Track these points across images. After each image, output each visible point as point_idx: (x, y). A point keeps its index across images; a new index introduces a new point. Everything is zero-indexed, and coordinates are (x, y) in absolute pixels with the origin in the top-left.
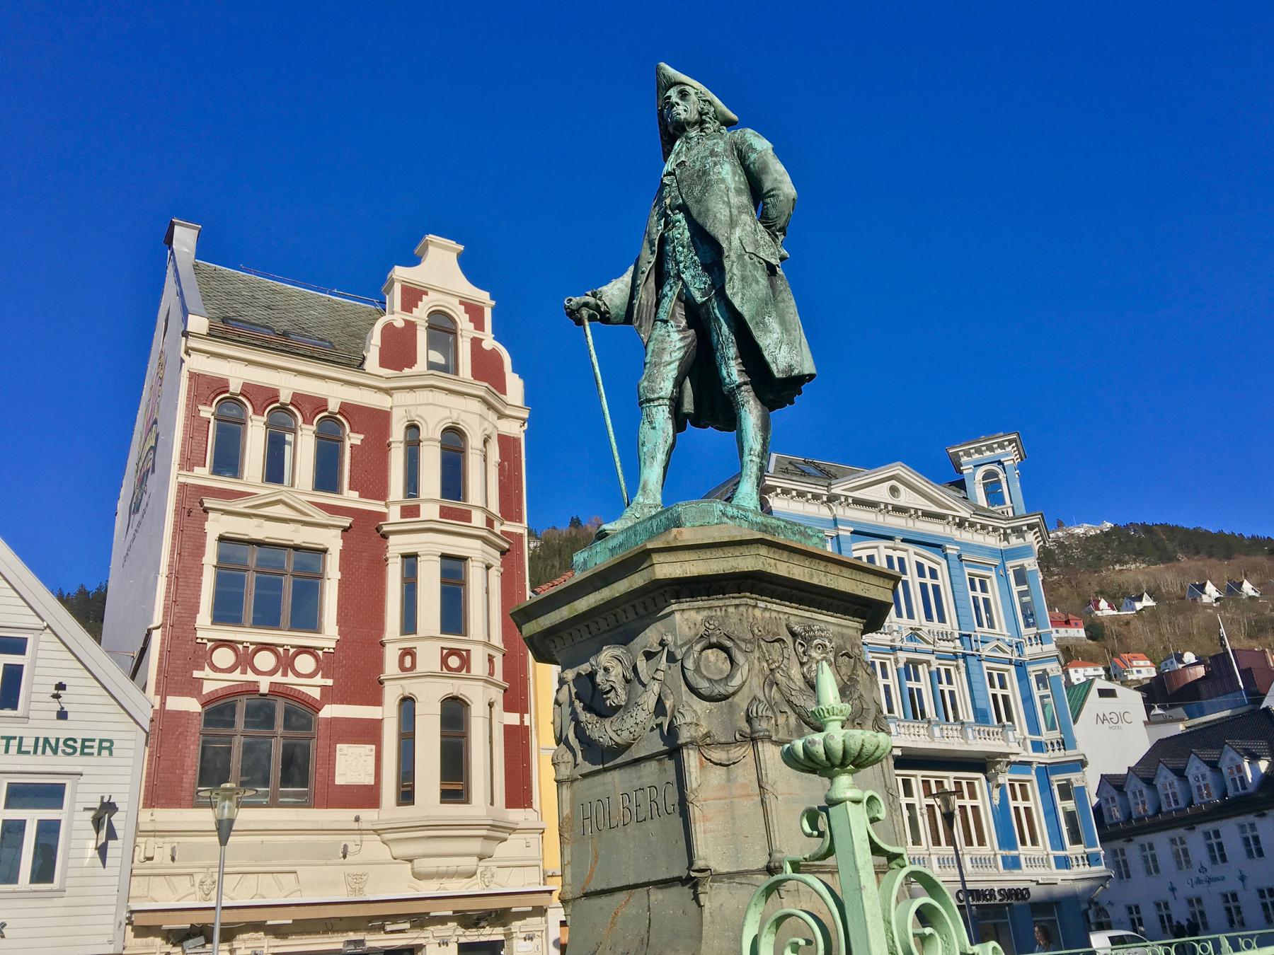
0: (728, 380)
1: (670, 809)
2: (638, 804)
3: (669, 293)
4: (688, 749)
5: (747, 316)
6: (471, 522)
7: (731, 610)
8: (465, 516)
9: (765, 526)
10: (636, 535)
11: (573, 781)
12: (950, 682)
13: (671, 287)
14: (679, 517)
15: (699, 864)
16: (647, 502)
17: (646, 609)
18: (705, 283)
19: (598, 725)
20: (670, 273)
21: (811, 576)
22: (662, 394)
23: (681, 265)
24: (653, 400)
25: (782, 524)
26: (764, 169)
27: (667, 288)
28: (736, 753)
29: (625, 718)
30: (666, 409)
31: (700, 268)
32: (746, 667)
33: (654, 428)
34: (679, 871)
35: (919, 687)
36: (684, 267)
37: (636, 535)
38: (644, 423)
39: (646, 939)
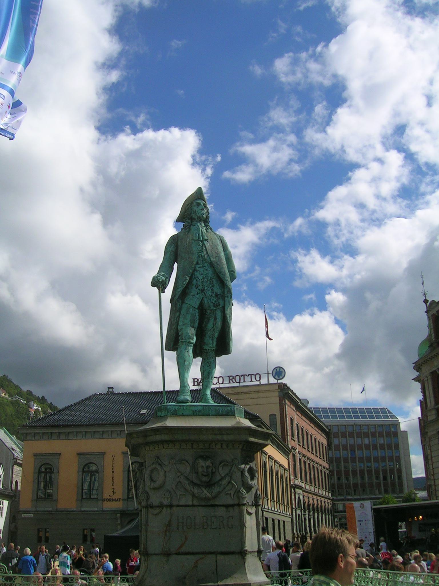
10: (209, 410)
13: (198, 294)
17: (227, 447)
18: (215, 301)
31: (214, 294)
39: (215, 572)
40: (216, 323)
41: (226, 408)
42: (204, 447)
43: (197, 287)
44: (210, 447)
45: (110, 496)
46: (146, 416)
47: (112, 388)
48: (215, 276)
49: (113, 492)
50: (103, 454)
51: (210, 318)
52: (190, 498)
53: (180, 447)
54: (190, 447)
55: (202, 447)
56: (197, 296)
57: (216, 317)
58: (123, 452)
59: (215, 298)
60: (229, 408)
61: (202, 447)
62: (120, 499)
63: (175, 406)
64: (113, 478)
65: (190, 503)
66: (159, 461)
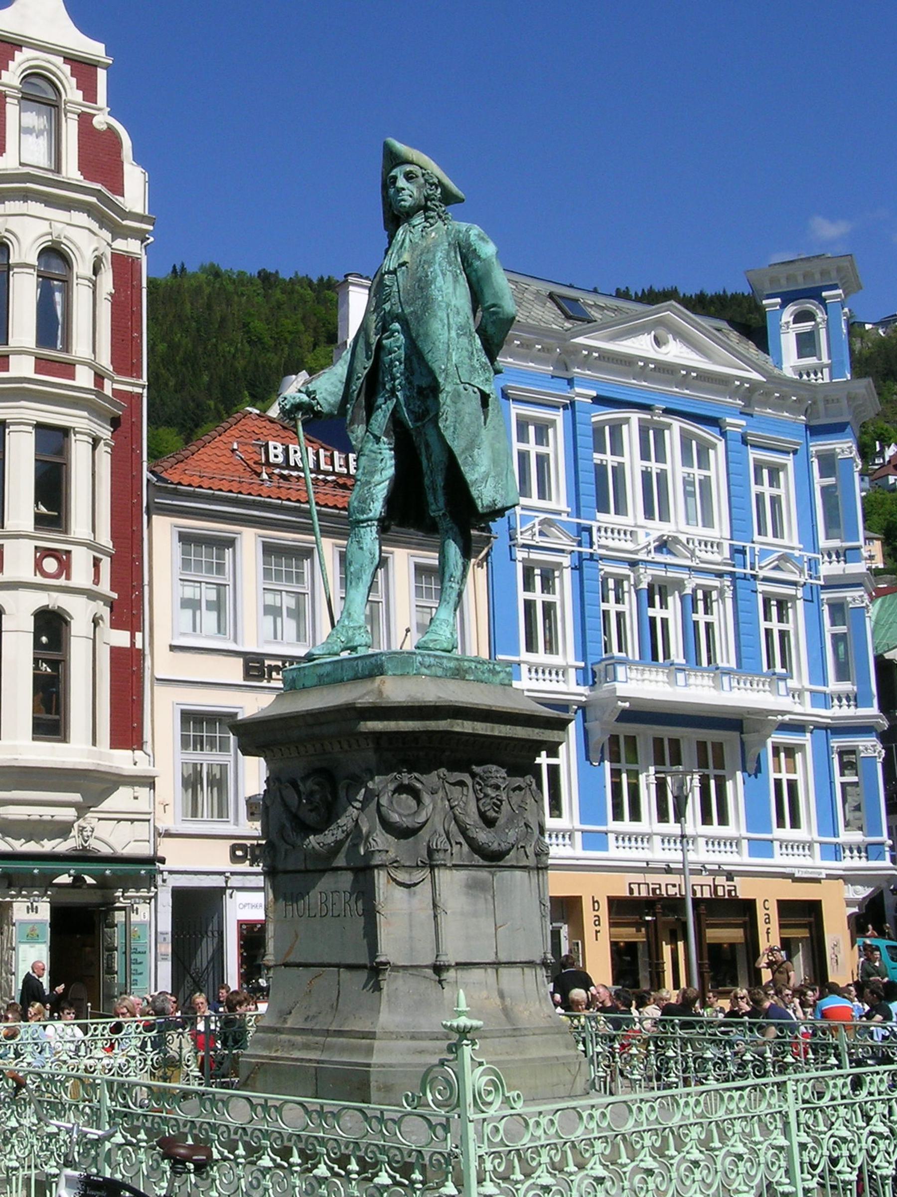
0: (433, 507)
3: (383, 406)
5: (457, 451)
6: (73, 378)
8: (67, 369)
9: (458, 670)
10: (342, 670)
12: (708, 610)
15: (382, 959)
16: (352, 625)
18: (419, 407)
20: (384, 385)
21: (492, 730)
22: (371, 515)
23: (397, 382)
24: (363, 521)
25: (473, 665)
26: (488, 274)
27: (380, 401)
28: (417, 875)
30: (374, 529)
32: (431, 807)
33: (361, 548)
34: (364, 960)
35: (665, 616)
37: (342, 670)
40: (431, 455)
57: (427, 440)
59: (419, 400)
65: (302, 867)
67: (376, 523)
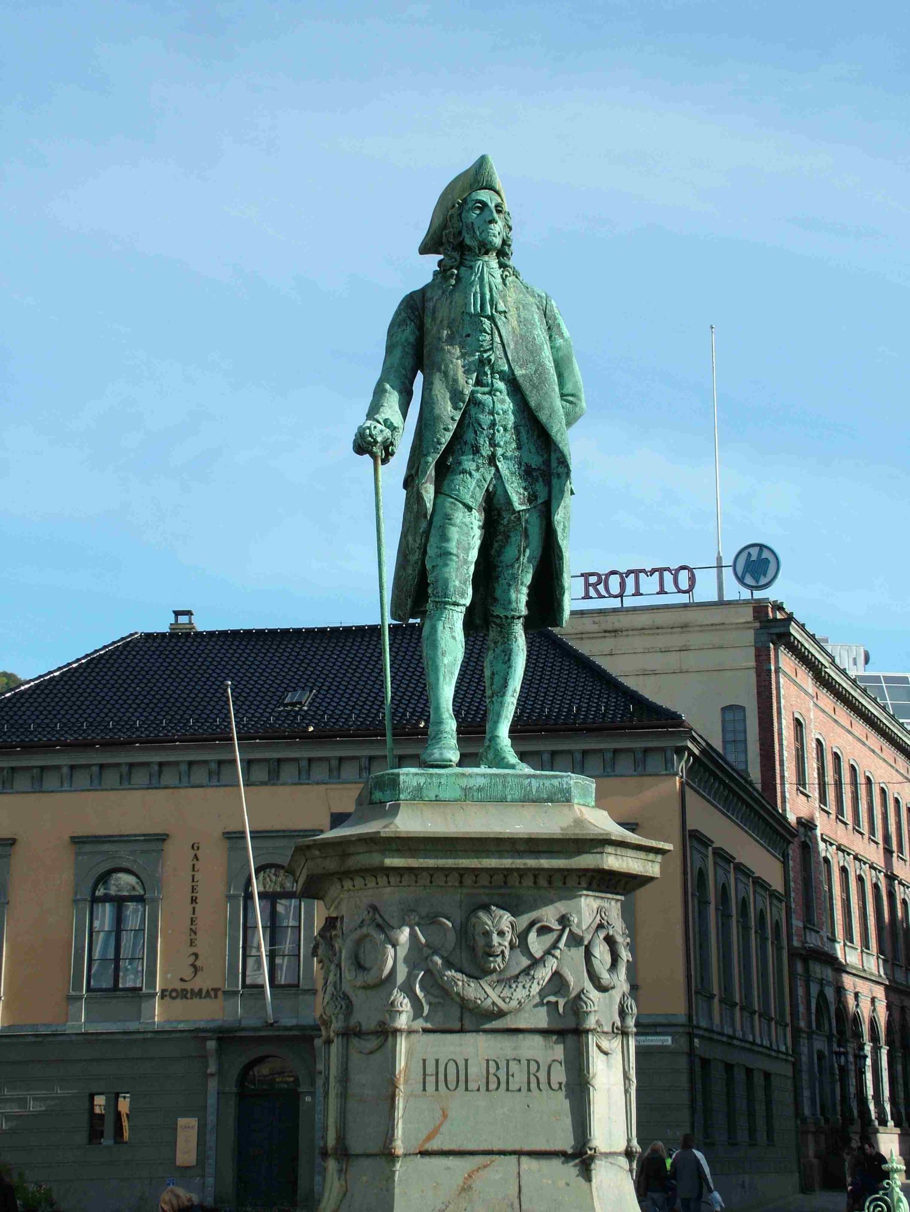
0: (514, 605)
1: (555, 1086)
2: (510, 1073)
4: (593, 1035)
7: (613, 903)
10: (504, 786)
11: (410, 1032)
14: (569, 791)
17: (550, 883)
19: (472, 985)
29: (514, 986)
36: (502, 455)
37: (504, 786)
38: (444, 628)
41: (547, 783)
42: (491, 883)
43: (476, 451)
44: (505, 883)
45: (182, 980)
46: (306, 711)
47: (189, 613)
48: (524, 418)
49: (193, 965)
50: (162, 838)
51: (512, 534)
52: (456, 1012)
53: (431, 882)
54: (457, 884)
55: (487, 884)
56: (477, 475)
58: (228, 833)
60: (555, 782)
61: (487, 884)
62: (216, 990)
63: (418, 777)
64: (192, 921)
66: (377, 916)
67: (464, 609)
